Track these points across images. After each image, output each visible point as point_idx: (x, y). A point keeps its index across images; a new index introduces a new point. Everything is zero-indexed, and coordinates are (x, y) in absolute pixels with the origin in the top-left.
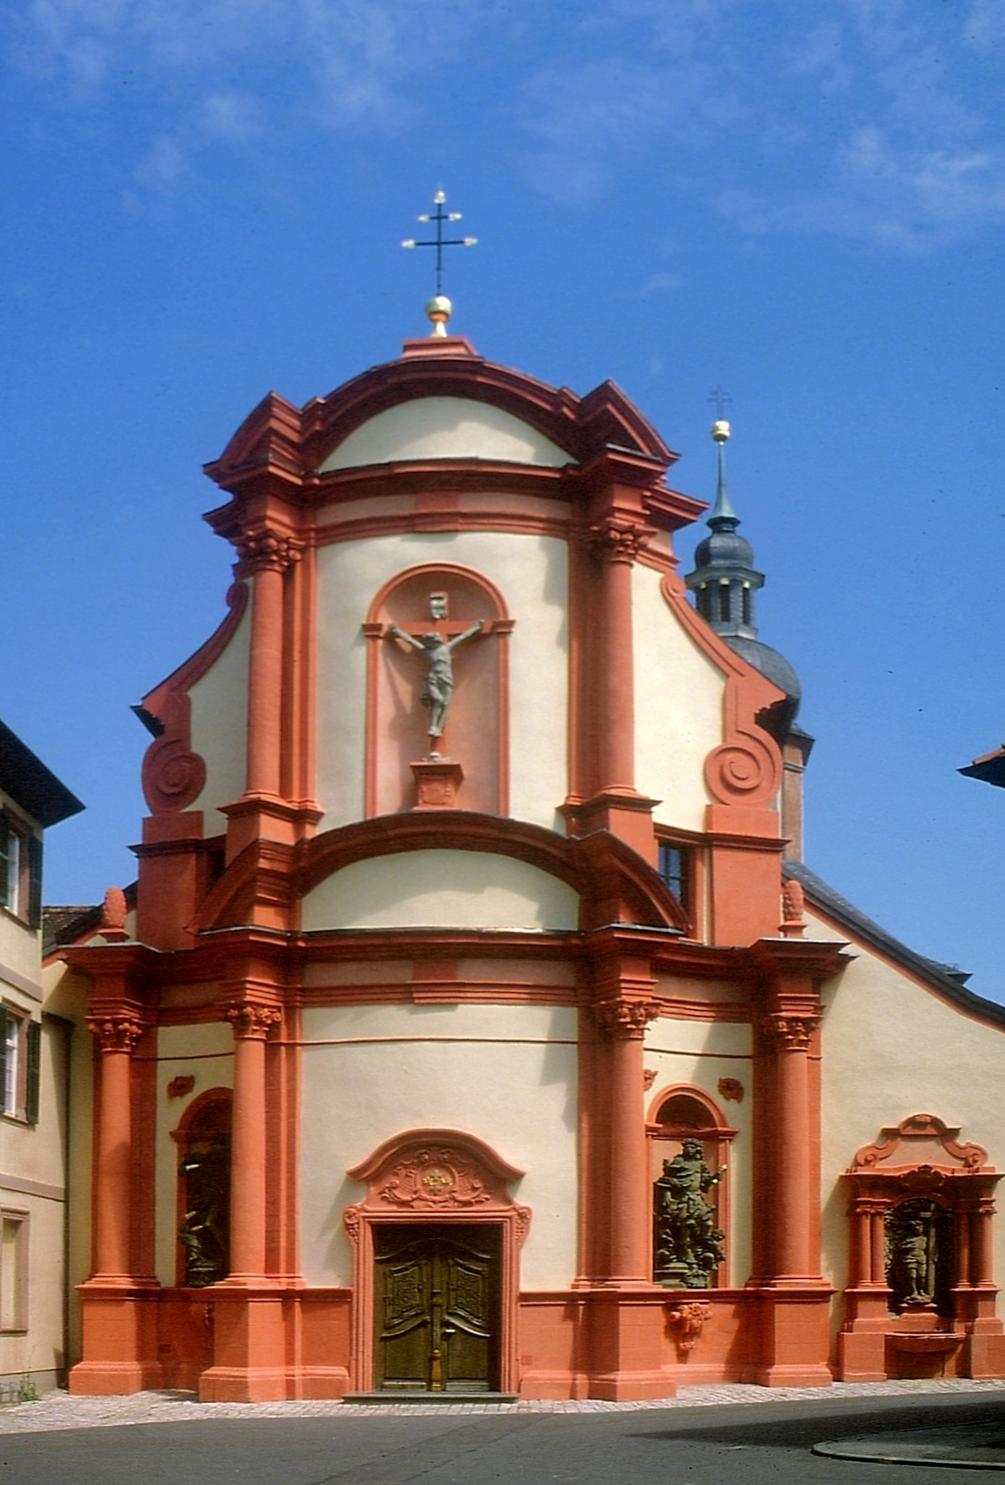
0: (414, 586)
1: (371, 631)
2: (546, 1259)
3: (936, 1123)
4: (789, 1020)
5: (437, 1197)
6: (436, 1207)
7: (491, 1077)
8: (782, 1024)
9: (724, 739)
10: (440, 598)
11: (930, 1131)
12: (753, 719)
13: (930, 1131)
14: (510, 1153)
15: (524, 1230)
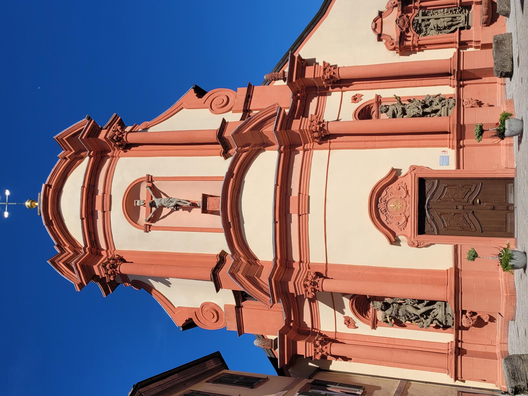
0: (131, 212)
1: (147, 229)
2: (437, 159)
3: (375, 21)
4: (325, 73)
5: (402, 206)
6: (409, 206)
7: (342, 183)
8: (326, 77)
9: (207, 108)
10: (136, 202)
11: (379, 21)
12: (199, 97)
13: (379, 21)
14: (383, 173)
15: (422, 168)
